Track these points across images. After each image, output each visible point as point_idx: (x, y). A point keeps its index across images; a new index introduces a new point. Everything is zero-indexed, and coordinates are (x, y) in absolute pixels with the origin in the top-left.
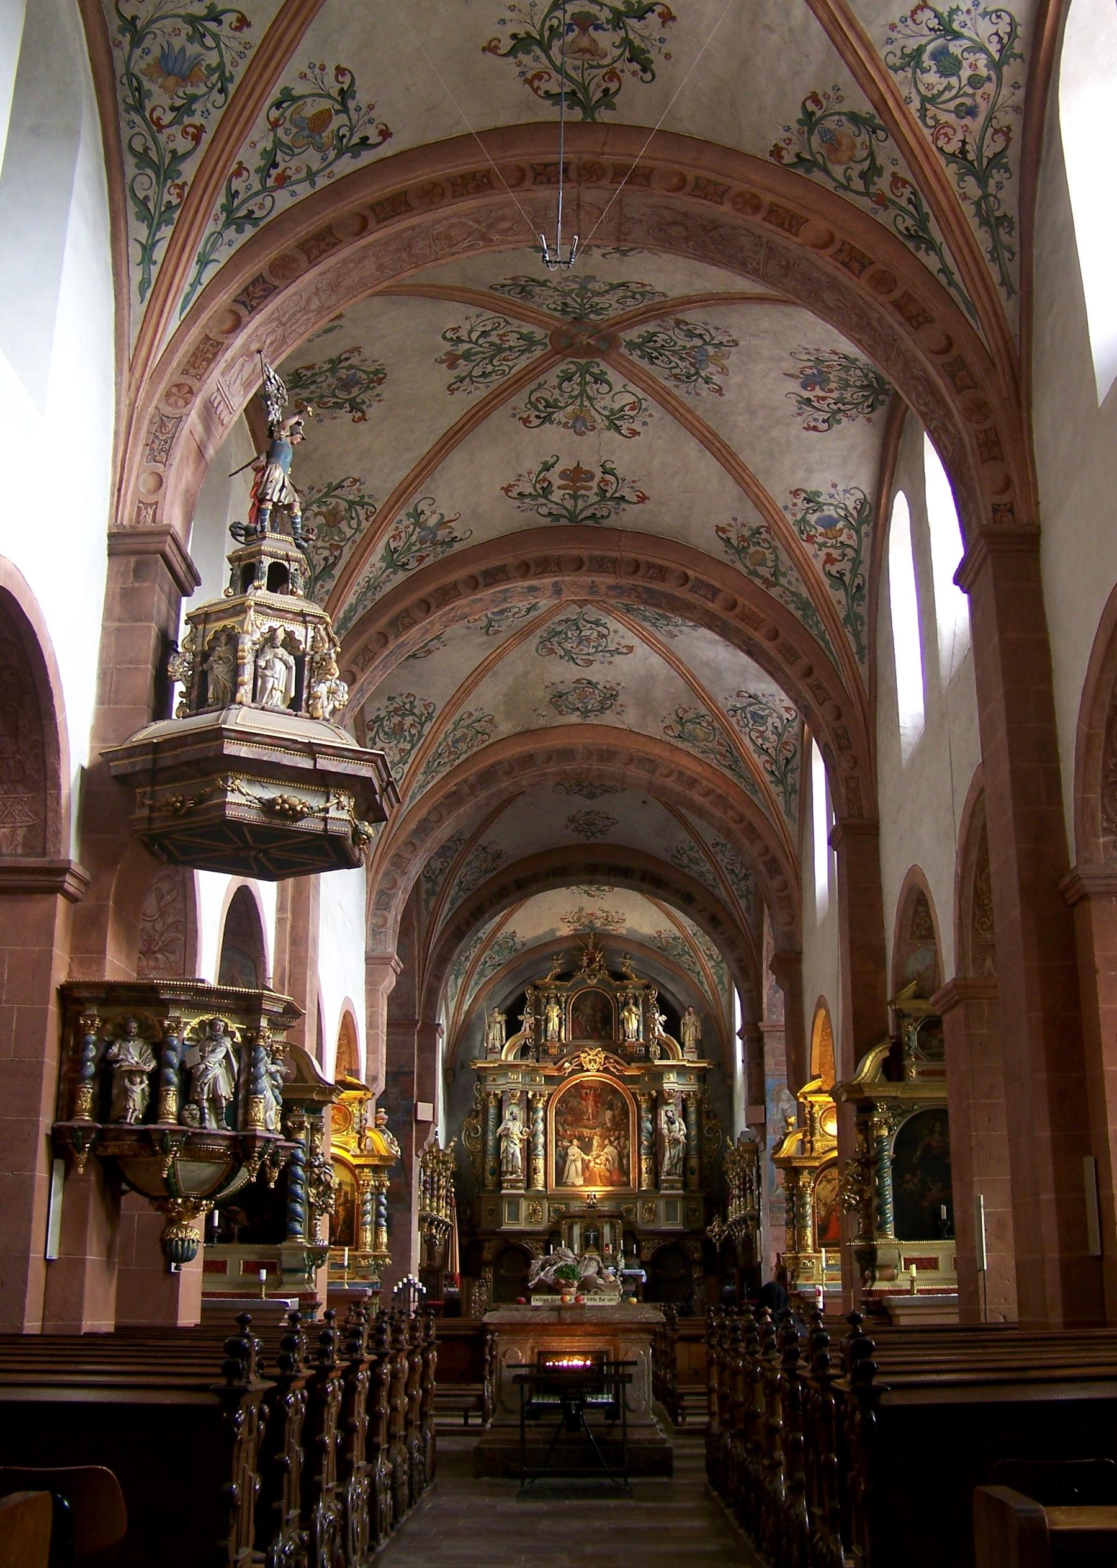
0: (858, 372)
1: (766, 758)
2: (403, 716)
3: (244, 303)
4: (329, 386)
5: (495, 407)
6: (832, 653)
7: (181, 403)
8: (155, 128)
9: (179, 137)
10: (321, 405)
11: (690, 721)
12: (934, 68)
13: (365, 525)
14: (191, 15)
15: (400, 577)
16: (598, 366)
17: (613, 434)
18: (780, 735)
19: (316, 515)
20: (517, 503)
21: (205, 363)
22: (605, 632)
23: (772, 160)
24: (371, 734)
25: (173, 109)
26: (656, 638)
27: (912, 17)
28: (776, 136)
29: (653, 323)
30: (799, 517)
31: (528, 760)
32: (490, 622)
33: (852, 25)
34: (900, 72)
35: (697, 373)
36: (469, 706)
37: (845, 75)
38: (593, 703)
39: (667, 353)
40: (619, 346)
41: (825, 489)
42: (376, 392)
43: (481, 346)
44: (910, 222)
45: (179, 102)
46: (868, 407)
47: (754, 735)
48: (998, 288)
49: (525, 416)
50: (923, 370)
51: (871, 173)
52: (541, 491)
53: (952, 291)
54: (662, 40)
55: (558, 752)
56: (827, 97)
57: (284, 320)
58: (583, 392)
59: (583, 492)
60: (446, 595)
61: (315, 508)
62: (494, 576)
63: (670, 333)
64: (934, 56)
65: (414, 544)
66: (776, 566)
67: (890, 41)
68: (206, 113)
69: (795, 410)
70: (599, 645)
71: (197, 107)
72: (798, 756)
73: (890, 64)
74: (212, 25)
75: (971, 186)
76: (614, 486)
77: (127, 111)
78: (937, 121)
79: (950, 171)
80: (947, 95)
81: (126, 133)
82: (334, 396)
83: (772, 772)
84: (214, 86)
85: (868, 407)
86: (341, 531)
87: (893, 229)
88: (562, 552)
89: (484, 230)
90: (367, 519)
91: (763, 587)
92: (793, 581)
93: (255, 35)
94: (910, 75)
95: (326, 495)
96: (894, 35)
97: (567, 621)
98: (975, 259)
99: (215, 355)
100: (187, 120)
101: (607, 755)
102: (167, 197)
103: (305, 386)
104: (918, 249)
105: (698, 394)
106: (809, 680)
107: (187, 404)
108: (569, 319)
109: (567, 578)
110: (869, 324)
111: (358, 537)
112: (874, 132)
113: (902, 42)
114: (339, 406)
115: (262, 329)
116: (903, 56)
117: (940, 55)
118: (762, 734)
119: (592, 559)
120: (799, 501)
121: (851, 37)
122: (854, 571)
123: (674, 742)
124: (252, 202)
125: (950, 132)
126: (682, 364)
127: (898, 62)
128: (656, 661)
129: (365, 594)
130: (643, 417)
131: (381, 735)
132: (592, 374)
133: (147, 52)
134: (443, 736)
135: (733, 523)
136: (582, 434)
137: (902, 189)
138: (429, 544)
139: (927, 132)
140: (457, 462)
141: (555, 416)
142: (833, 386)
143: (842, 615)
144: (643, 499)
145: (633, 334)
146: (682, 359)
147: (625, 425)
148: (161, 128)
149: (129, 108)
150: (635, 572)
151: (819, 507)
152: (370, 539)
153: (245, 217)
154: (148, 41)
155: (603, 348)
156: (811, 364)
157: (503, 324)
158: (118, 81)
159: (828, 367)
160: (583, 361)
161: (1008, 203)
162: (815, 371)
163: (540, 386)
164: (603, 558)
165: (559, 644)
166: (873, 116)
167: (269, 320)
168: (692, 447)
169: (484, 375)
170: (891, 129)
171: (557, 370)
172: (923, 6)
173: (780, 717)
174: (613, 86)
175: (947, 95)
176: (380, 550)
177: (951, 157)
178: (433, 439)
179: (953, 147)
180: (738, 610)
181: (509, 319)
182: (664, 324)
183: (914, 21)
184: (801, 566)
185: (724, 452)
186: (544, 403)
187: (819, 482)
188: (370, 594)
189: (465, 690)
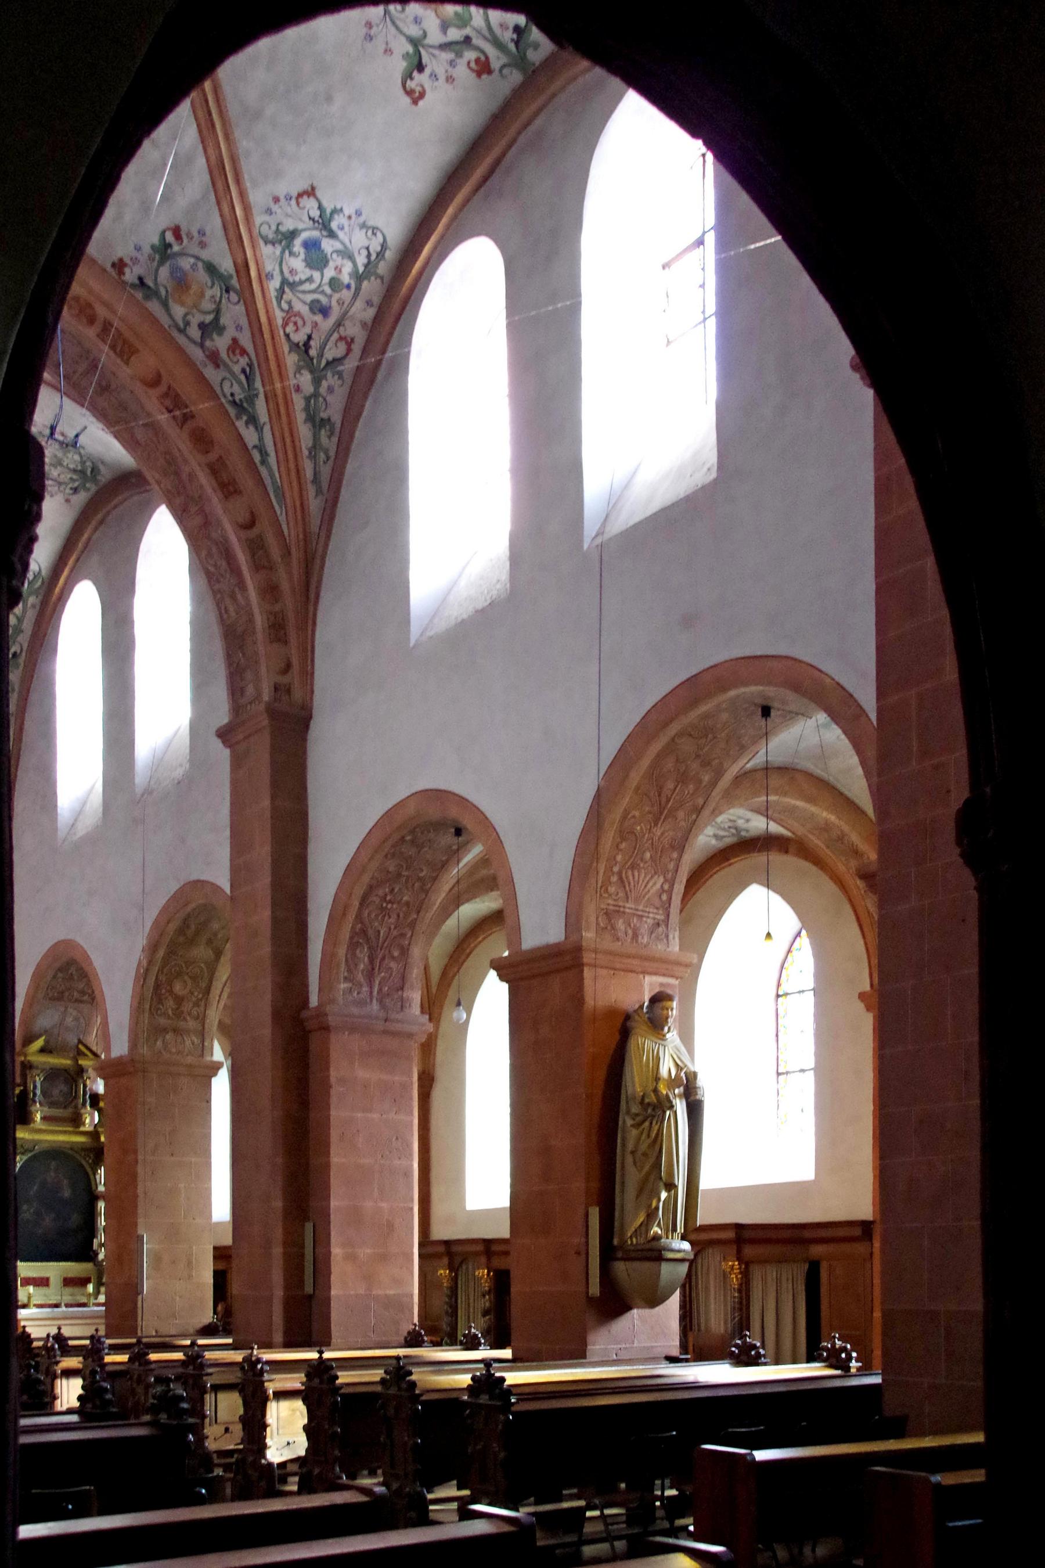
0: (77, 457)
12: (302, 256)
28: (123, 251)
33: (238, 181)
34: (270, 247)
37: (214, 224)
44: (236, 389)
46: (71, 489)
51: (211, 328)
53: (263, 471)
56: (190, 237)
64: (306, 245)
67: (269, 211)
75: (306, 379)
78: (291, 307)
79: (291, 360)
80: (307, 287)
87: (219, 391)
94: (278, 252)
96: (275, 208)
98: (294, 448)
104: (238, 417)
112: (227, 291)
116: (277, 231)
117: (311, 246)
125: (300, 323)
127: (271, 236)
137: (239, 357)
139: (279, 316)
166: (231, 277)
170: (247, 297)
177: (295, 347)
179: (299, 337)
183: (298, 204)
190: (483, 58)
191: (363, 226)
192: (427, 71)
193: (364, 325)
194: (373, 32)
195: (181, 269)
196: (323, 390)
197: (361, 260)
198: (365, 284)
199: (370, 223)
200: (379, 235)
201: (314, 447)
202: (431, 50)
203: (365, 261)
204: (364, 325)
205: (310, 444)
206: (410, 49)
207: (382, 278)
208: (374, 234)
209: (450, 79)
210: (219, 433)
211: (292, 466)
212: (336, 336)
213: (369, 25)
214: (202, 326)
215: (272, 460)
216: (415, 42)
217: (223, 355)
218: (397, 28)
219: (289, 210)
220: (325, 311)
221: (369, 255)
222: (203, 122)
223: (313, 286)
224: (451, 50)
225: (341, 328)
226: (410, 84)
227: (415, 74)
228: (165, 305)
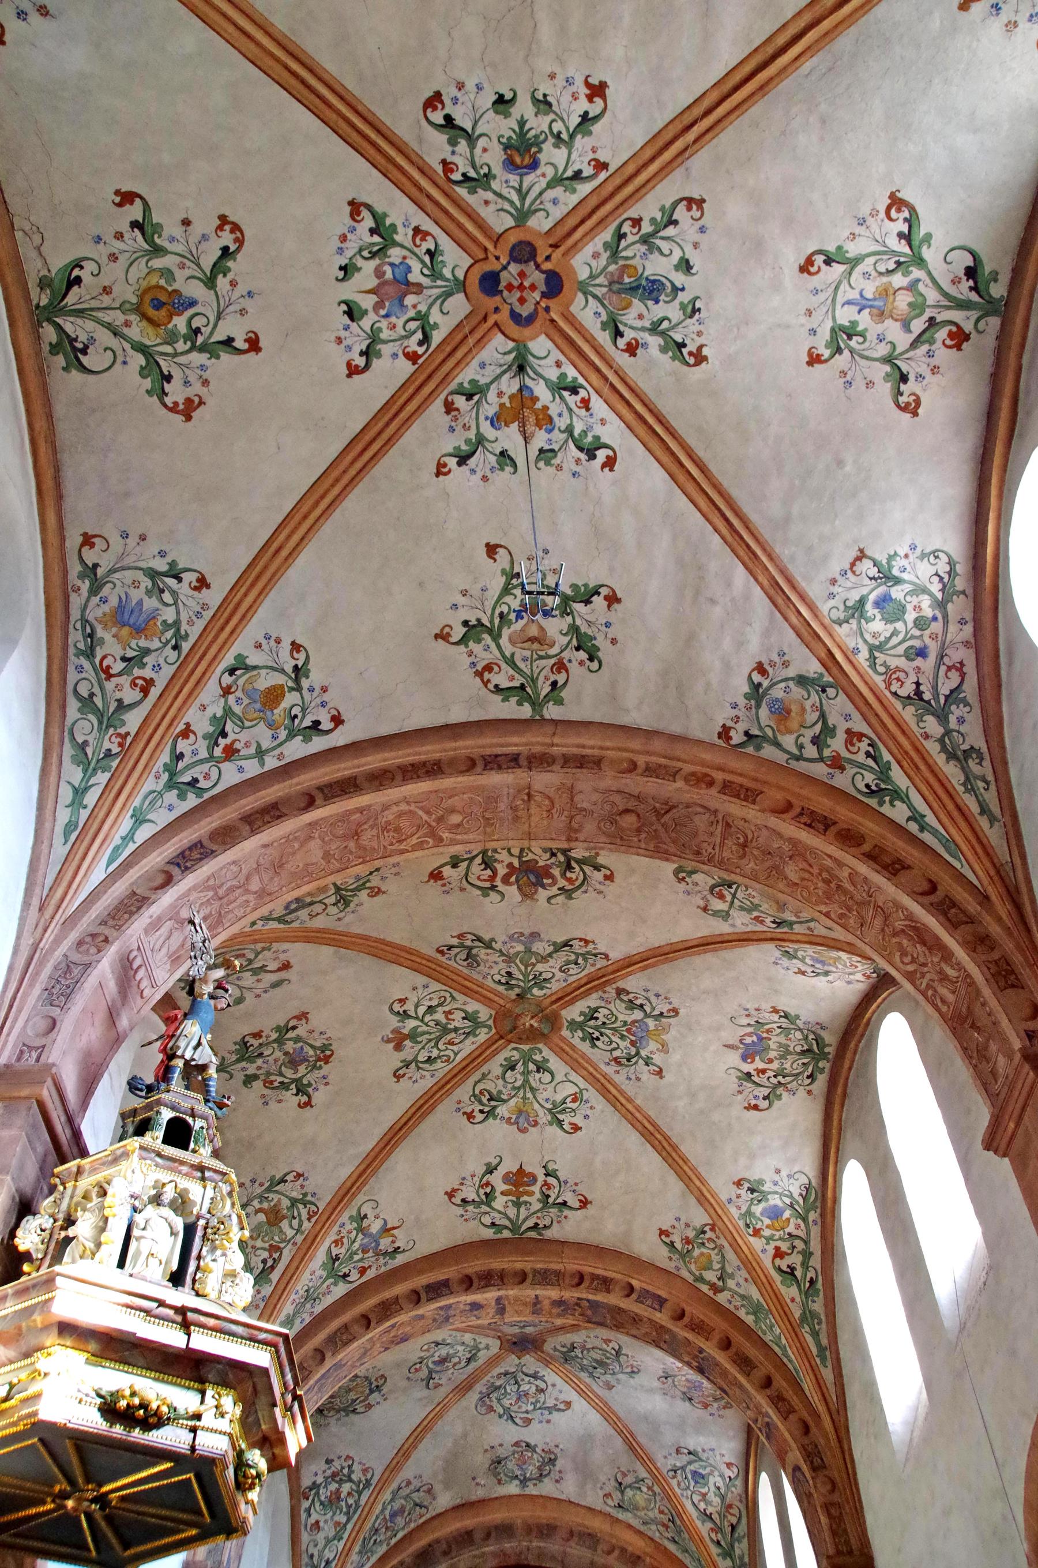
0: (799, 1035)
1: (709, 1525)
2: (341, 1482)
3: (178, 865)
4: (276, 1061)
5: (439, 1101)
6: (790, 1361)
7: (93, 950)
8: (103, 676)
9: (127, 685)
10: (268, 1084)
11: (630, 1486)
12: (879, 617)
14: (151, 569)
15: (340, 1290)
17: (555, 1129)
18: (723, 1498)
19: (257, 1211)
20: (460, 1211)
21: (126, 916)
22: (543, 1385)
23: (721, 742)
24: (306, 1504)
25: (124, 659)
26: (593, 1392)
27: (851, 569)
29: (595, 996)
30: (744, 1209)
31: (466, 1538)
32: (430, 1372)
33: (794, 587)
34: (845, 625)
35: (637, 1054)
36: (408, 1472)
38: (531, 1470)
39: (608, 1032)
40: (560, 1029)
41: (768, 1176)
42: (322, 1072)
43: (427, 1025)
44: (870, 778)
45: (130, 654)
46: (808, 1077)
47: (696, 1498)
48: (978, 818)
49: (469, 1110)
50: (910, 917)
52: (484, 1197)
53: (927, 837)
54: (608, 625)
55: (496, 1527)
57: (221, 892)
58: (526, 1082)
59: (525, 1198)
60: (387, 1309)
61: (256, 1203)
62: (437, 1290)
63: (611, 1006)
64: (878, 604)
65: (356, 1253)
66: (723, 1268)
67: (832, 596)
68: (157, 668)
69: (735, 1087)
70: (537, 1401)
71: (149, 660)
72: (744, 1521)
73: (834, 618)
74: (171, 582)
76: (556, 1191)
77: (77, 656)
78: (887, 667)
79: (908, 714)
80: (895, 640)
81: (72, 676)
82: (281, 1074)
83: (718, 1543)
84: (168, 642)
85: (808, 1077)
86: (281, 1231)
88: (505, 1266)
89: (434, 824)
90: (309, 1219)
91: (711, 1293)
92: (742, 1282)
93: (214, 597)
95: (269, 1190)
96: (835, 589)
97: (506, 1374)
99: (139, 908)
100: (137, 672)
101: (546, 1530)
102: (107, 745)
103: (251, 1060)
104: (881, 803)
105: (638, 1079)
106: (768, 1392)
107: (99, 951)
108: (512, 994)
109: (511, 1292)
110: (839, 887)
111: (299, 1239)
112: (824, 691)
113: (844, 595)
114: (284, 1086)
115: (194, 896)
117: (882, 602)
118: (704, 1495)
119: (535, 1272)
120: (743, 1192)
121: (794, 598)
122: (805, 1265)
123: (614, 1512)
124: (198, 769)
125: (902, 675)
126: (623, 1044)
128: (594, 1418)
129: (303, 1304)
130: (584, 1110)
131: (317, 1504)
132: (535, 1062)
133: (104, 601)
134: (380, 1507)
135: (676, 1224)
136: (523, 1131)
137: (858, 744)
138: (371, 1254)
139: (879, 680)
140: (401, 1159)
141: (498, 1110)
142: (772, 1054)
143: (797, 1314)
144: (585, 1203)
146: (622, 1037)
147: (567, 1119)
148: (109, 676)
149: (80, 653)
150: (579, 1284)
151: (764, 1197)
152: (311, 1242)
153: (188, 784)
154: (106, 590)
155: (546, 1031)
156: (750, 1030)
158: (71, 626)
159: (768, 1031)
160: (526, 1047)
161: (973, 735)
162: (755, 1038)
164: (546, 1271)
165: (499, 1400)
166: (821, 675)
167: (204, 886)
168: (633, 1139)
169: (430, 1060)
171: (500, 1058)
172: (861, 556)
173: (722, 1476)
174: (561, 678)
175: (895, 640)
176: (320, 1256)
179: (908, 689)
180: (686, 1320)
182: (606, 996)
183: (854, 572)
184: (749, 1264)
185: (666, 1144)
187: (761, 1170)
188: (308, 1306)
189: (404, 1453)
190: (954, 329)
191: (923, 556)
192: (912, 377)
193: (966, 644)
194: (848, 378)
195: (777, 700)
196: (953, 723)
197: (935, 588)
198: (950, 606)
199: (927, 551)
200: (941, 555)
201: (967, 778)
202: (906, 356)
203: (940, 586)
204: (966, 644)
205: (962, 779)
206: (888, 368)
207: (963, 592)
208: (936, 557)
209: (935, 370)
210: (869, 826)
211: (951, 806)
212: (943, 668)
213: (844, 374)
214: (815, 741)
215: (931, 819)
216: (888, 360)
217: (845, 754)
218: (867, 358)
219: (849, 585)
220: (922, 653)
221: (941, 579)
222: (746, 558)
223: (901, 637)
224: (923, 343)
225: (946, 660)
226: (902, 400)
227: (903, 387)
228: (777, 745)
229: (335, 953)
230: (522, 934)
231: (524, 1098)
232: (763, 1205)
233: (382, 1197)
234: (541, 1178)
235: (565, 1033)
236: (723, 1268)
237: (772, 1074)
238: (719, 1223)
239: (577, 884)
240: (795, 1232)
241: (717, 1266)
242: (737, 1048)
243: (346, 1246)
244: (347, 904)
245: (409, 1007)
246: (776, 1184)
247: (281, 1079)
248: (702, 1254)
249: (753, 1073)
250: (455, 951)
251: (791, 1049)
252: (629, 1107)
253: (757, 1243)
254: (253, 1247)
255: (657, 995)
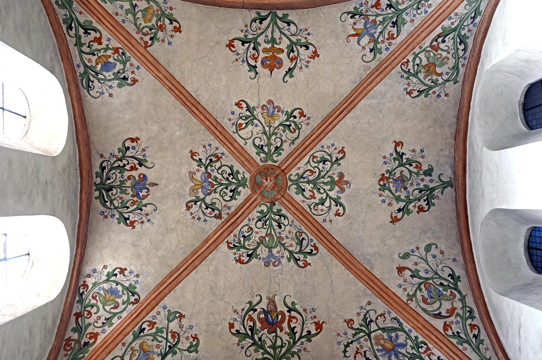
10: (419, 166)
13: (410, 58)
16: (261, 159)
19: (441, 75)
29: (233, 209)
35: (206, 168)
41: (115, 91)
42: (386, 167)
49: (302, 118)
58: (269, 139)
59: (269, 46)
63: (224, 203)
66: (134, 15)
82: (410, 172)
86: (428, 58)
90: (408, 61)
92: (120, 12)
105: (204, 147)
111: (417, 50)
120: (131, 76)
126: (215, 174)
130: (234, 118)
132: (264, 152)
136: (270, 102)
141: (285, 118)
145: (245, 192)
155: (258, 176)
157: (312, 207)
159: (134, 203)
160: (270, 162)
162: (141, 194)
163: (293, 142)
168: (204, 99)
169: (324, 161)
171: (284, 155)
178: (356, 111)
181: (308, 210)
186: (291, 128)
229: (372, 268)
230: (274, 266)
231: (270, 127)
232: (116, 70)
233: (358, 63)
234: (259, 64)
235: (248, 175)
236: (134, 15)
237: (127, 167)
238: (142, 50)
239: (247, 317)
240: (90, 56)
241: (139, 15)
242: (149, 184)
243: (387, 32)
244: (365, 319)
245: (334, 208)
246: (111, 87)
247: (411, 168)
248: (150, 21)
249: (138, 166)
250: (308, 250)
251: (119, 190)
252: (208, 123)
253: (115, 44)
254: (449, 53)
255: (199, 219)
